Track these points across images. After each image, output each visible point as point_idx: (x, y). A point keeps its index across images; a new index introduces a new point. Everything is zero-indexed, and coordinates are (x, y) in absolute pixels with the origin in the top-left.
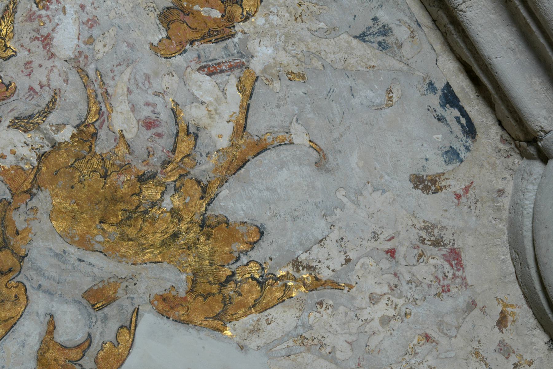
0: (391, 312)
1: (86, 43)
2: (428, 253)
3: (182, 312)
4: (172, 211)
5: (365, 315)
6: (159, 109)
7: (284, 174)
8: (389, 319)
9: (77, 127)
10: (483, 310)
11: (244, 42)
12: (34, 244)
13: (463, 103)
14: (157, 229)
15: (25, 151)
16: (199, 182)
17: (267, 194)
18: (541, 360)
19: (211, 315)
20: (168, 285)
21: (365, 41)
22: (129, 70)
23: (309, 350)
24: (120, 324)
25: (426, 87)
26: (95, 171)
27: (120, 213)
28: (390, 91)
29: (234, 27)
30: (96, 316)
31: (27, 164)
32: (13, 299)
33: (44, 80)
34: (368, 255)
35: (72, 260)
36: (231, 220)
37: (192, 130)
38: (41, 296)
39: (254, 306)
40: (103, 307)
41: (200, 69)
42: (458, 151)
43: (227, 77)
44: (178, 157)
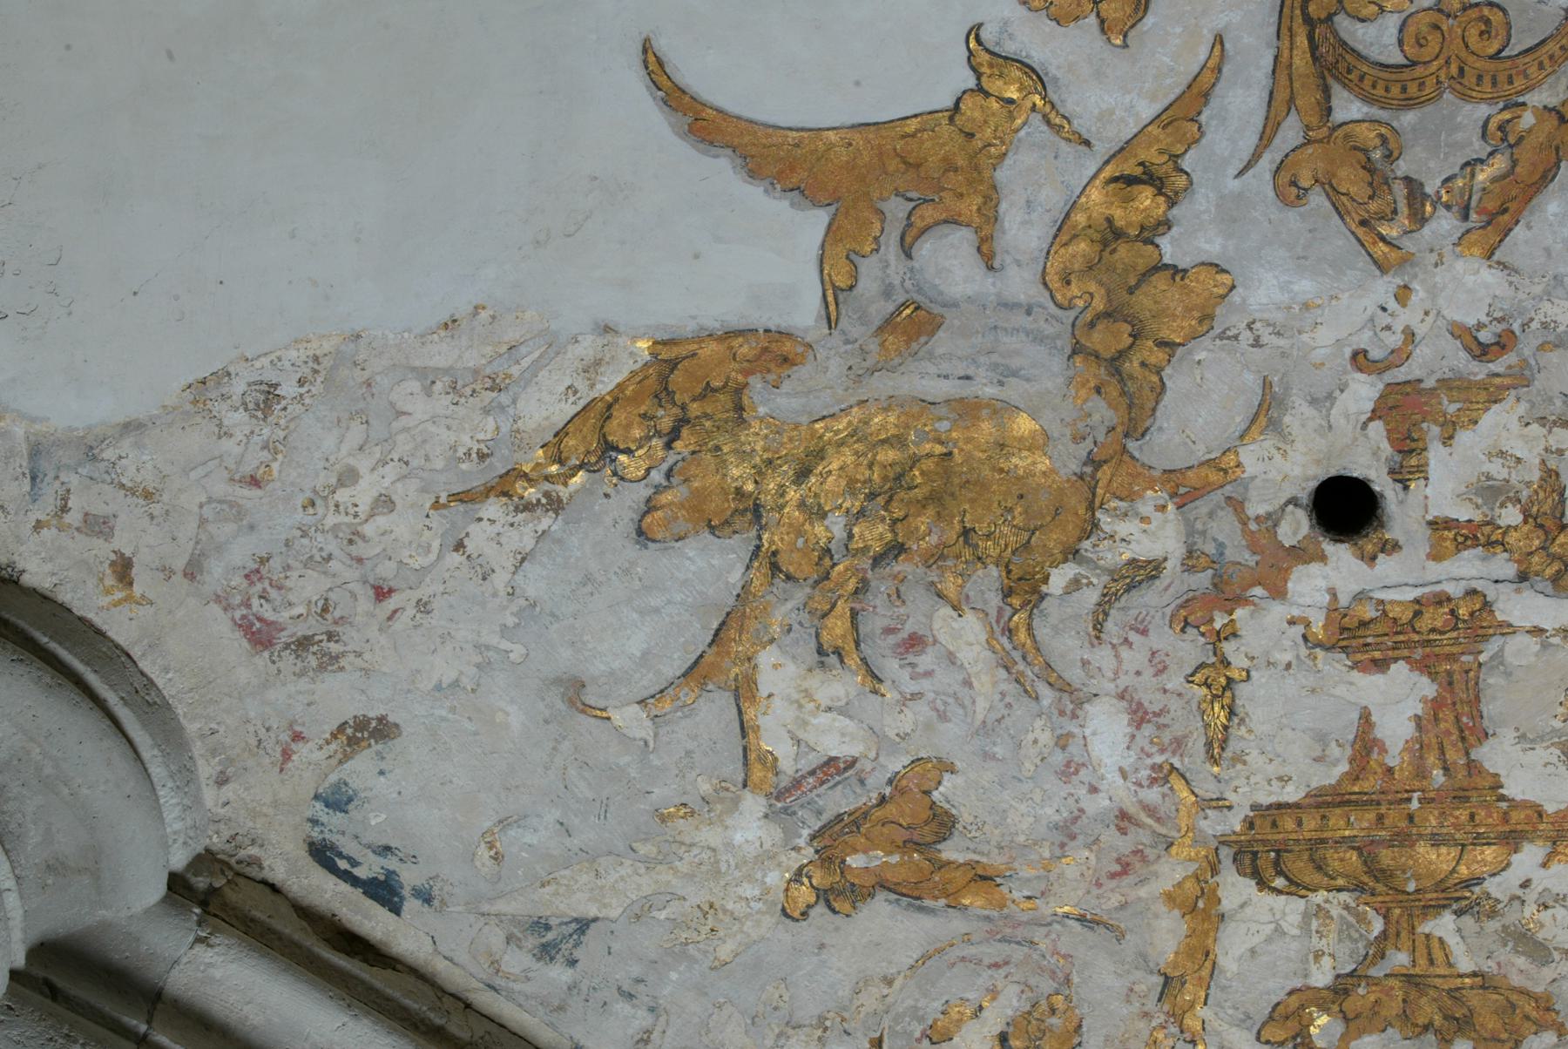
0: (342, 495)
1: (1070, 735)
2: (312, 621)
3: (745, 349)
4: (823, 515)
5: (391, 471)
6: (905, 675)
7: (636, 645)
8: (341, 483)
9: (1043, 597)
10: (167, 572)
11: (789, 834)
12: (1060, 380)
13: (357, 893)
14: (840, 476)
15: (1123, 528)
16: (789, 577)
17: (655, 600)
18: (19, 540)
19: (686, 363)
20: (786, 386)
21: (576, 920)
22: (980, 717)
23: (476, 372)
24: (855, 292)
25: (436, 892)
26: (988, 536)
28: (497, 858)
29: (817, 852)
30: (907, 292)
31: (1115, 509)
32: (1073, 277)
33: (1125, 653)
34: (424, 570)
35: (982, 374)
36: (706, 536)
37: (833, 659)
38: (1022, 297)
39: (610, 407)
40: (899, 311)
41: (852, 763)
42: (331, 811)
43: (799, 767)
44: (842, 607)
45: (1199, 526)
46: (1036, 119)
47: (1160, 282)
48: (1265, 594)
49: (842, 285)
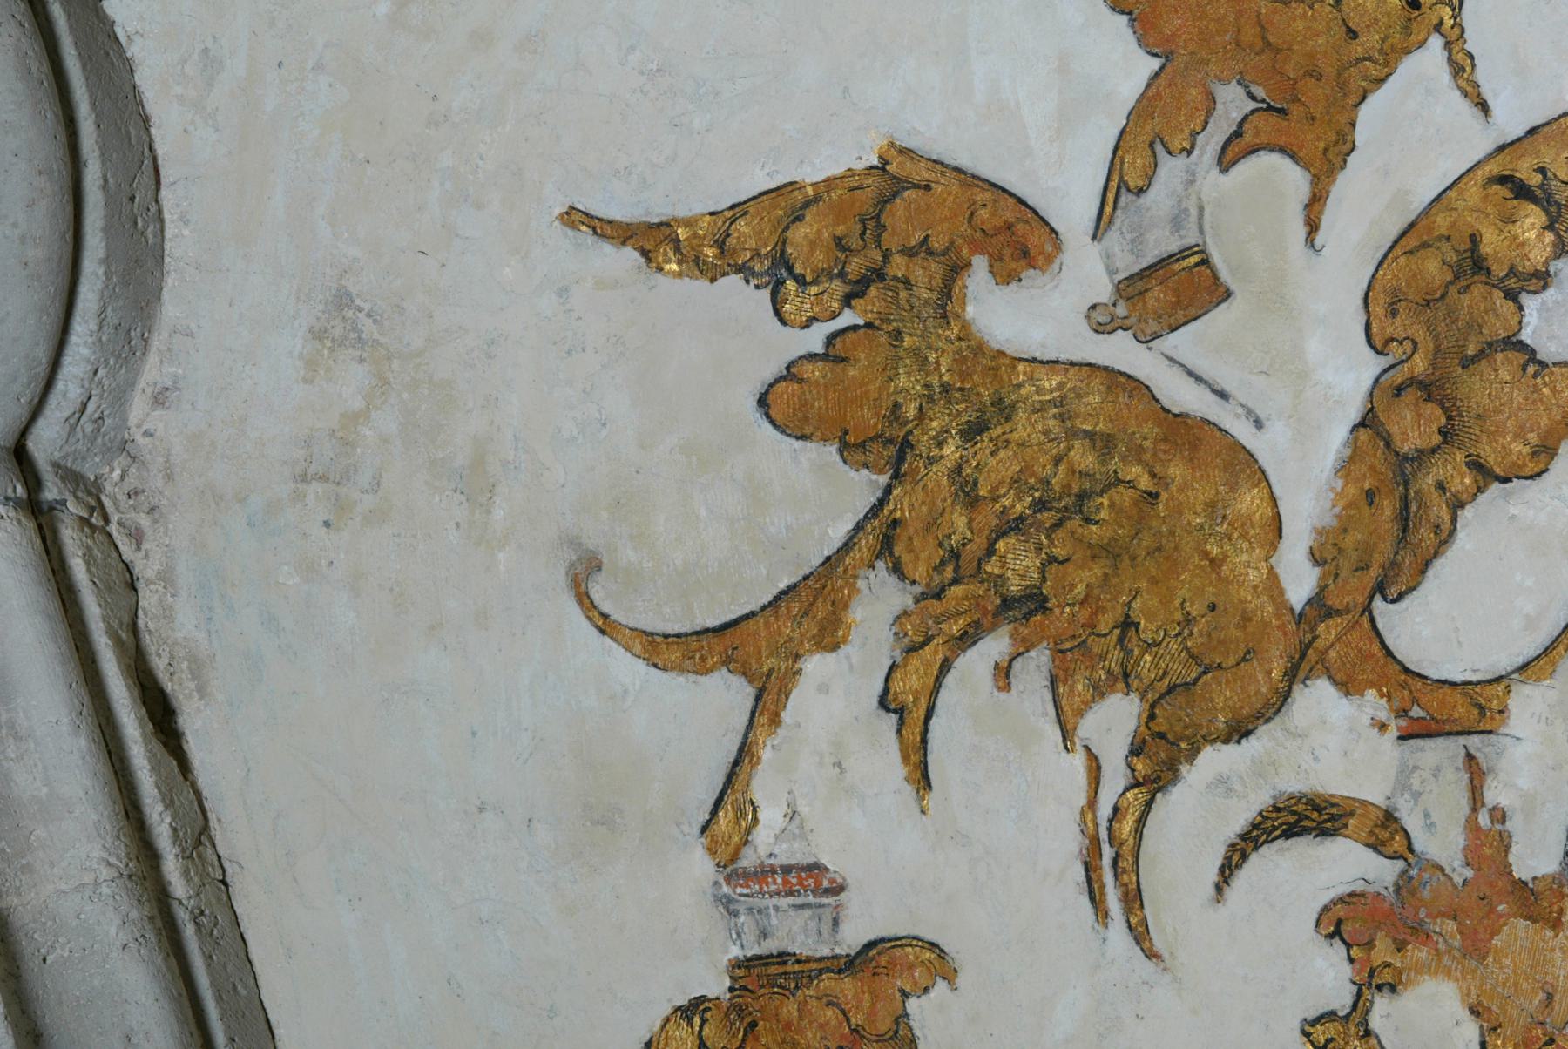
27: (1104, 514)
29: (731, 989)
36: (832, 450)
39: (807, 204)
43: (776, 851)
45: (1415, 782)
46: (1436, 42)
47: (1505, 367)
48: (1457, 941)
49: (1132, 185)
